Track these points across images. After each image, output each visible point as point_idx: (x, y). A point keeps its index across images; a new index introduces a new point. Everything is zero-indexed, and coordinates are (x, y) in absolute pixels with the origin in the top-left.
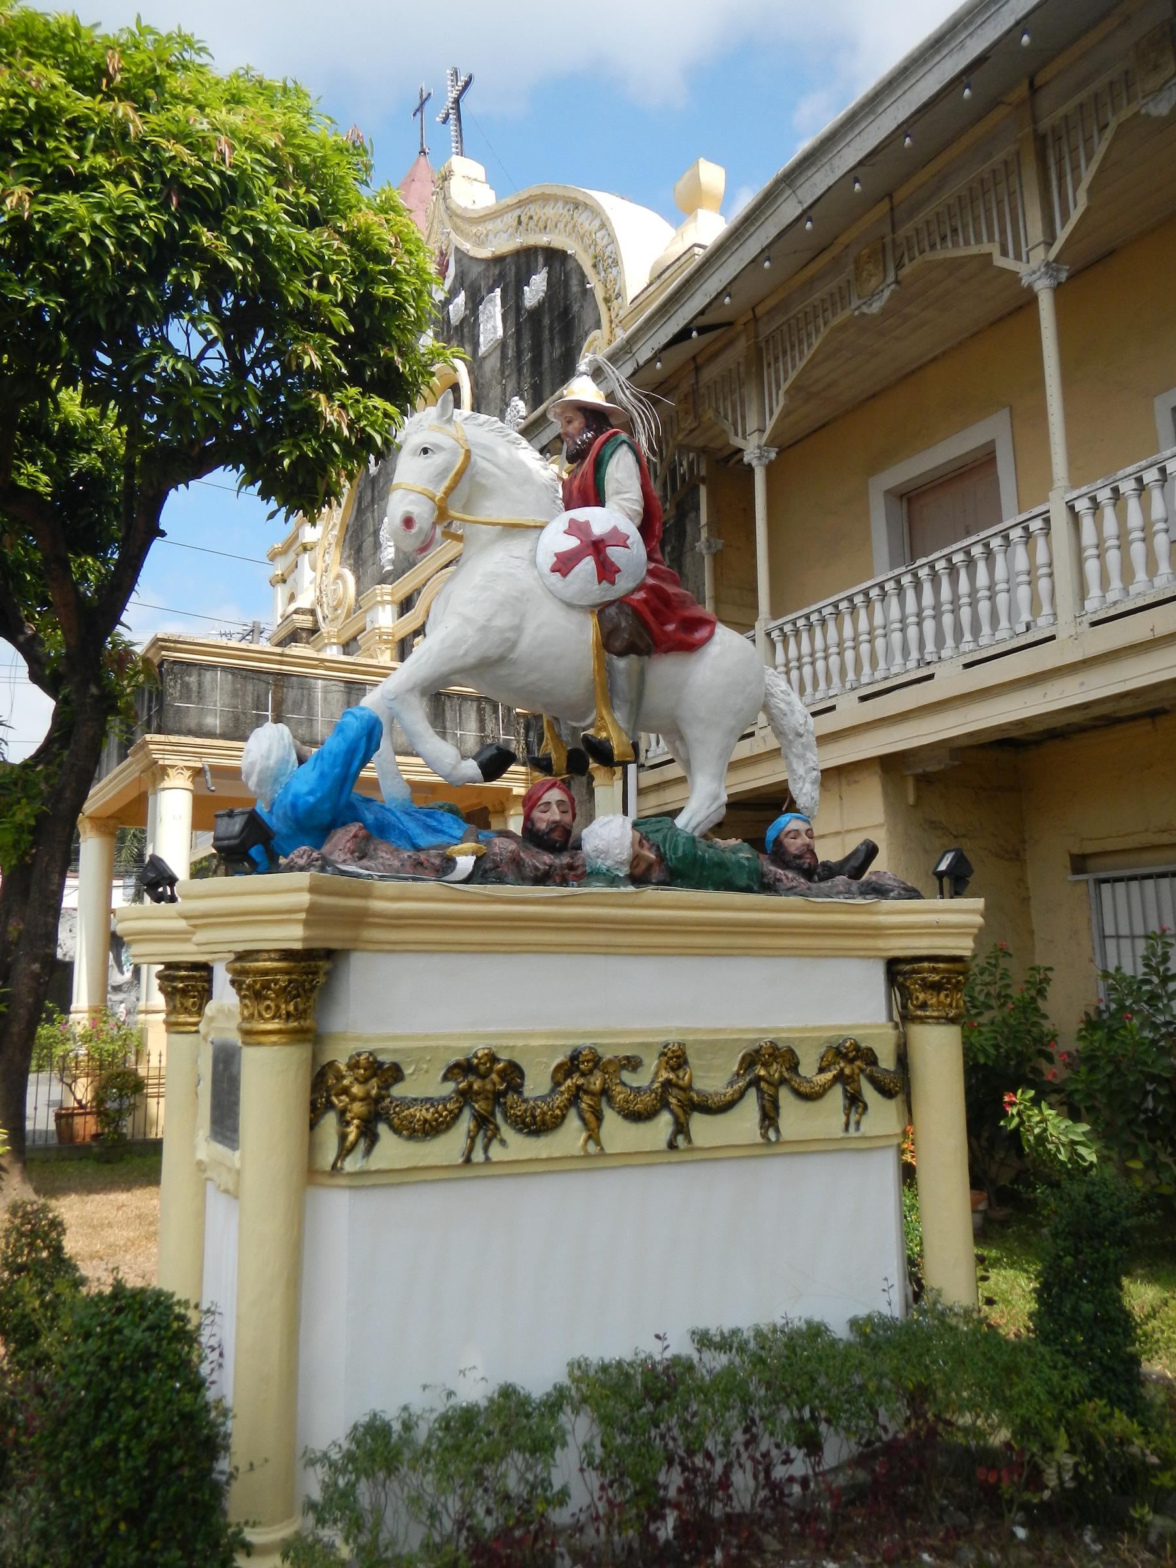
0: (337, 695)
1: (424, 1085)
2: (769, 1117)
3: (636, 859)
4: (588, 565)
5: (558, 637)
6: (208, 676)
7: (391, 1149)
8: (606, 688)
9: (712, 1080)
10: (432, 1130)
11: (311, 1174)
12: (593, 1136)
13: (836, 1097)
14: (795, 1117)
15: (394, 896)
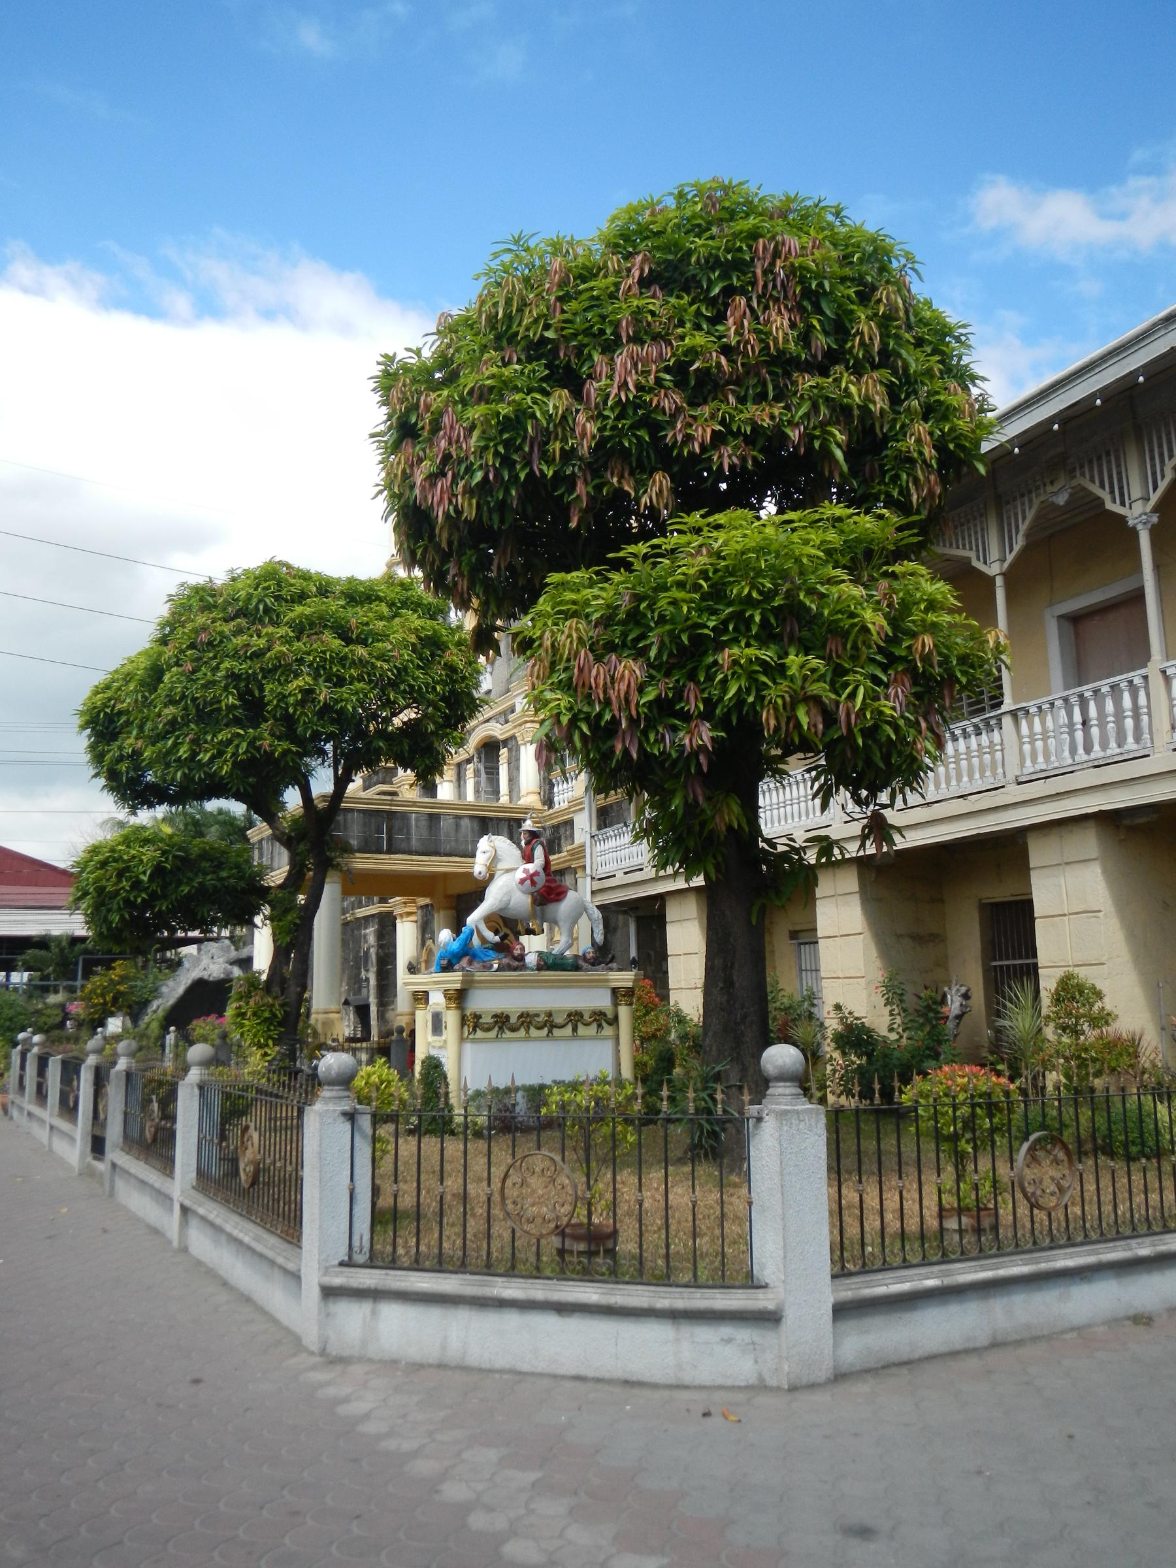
0: (424, 823)
1: (487, 1019)
2: (575, 1029)
3: (538, 965)
4: (528, 882)
5: (521, 901)
6: (349, 816)
7: (480, 1034)
8: (534, 915)
9: (559, 1020)
10: (488, 1030)
11: (462, 1040)
12: (527, 1032)
13: (595, 1025)
14: (582, 1030)
15: (479, 976)
